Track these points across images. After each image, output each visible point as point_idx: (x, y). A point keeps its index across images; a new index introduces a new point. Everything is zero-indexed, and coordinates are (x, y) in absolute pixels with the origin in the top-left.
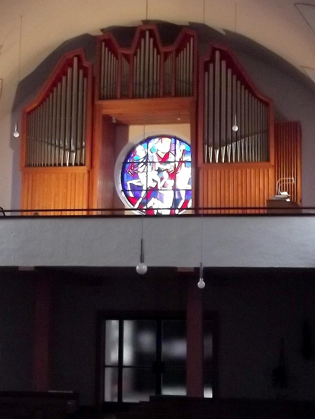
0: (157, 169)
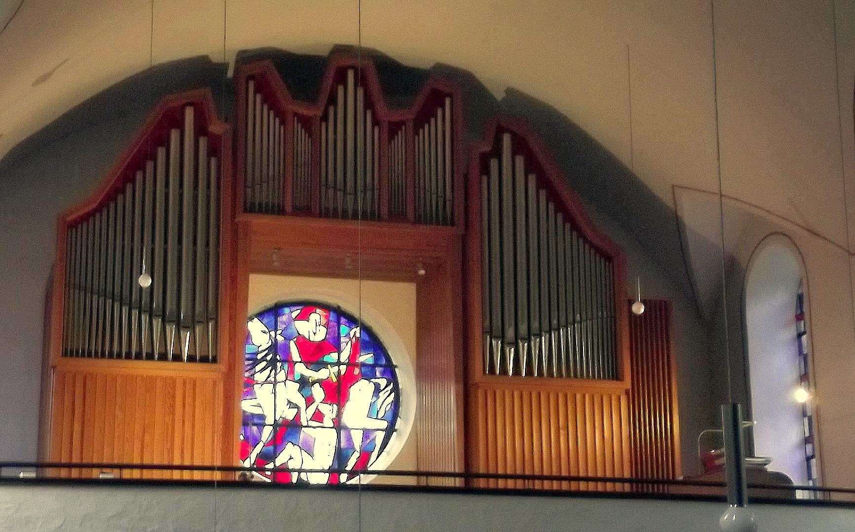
0: (297, 378)
